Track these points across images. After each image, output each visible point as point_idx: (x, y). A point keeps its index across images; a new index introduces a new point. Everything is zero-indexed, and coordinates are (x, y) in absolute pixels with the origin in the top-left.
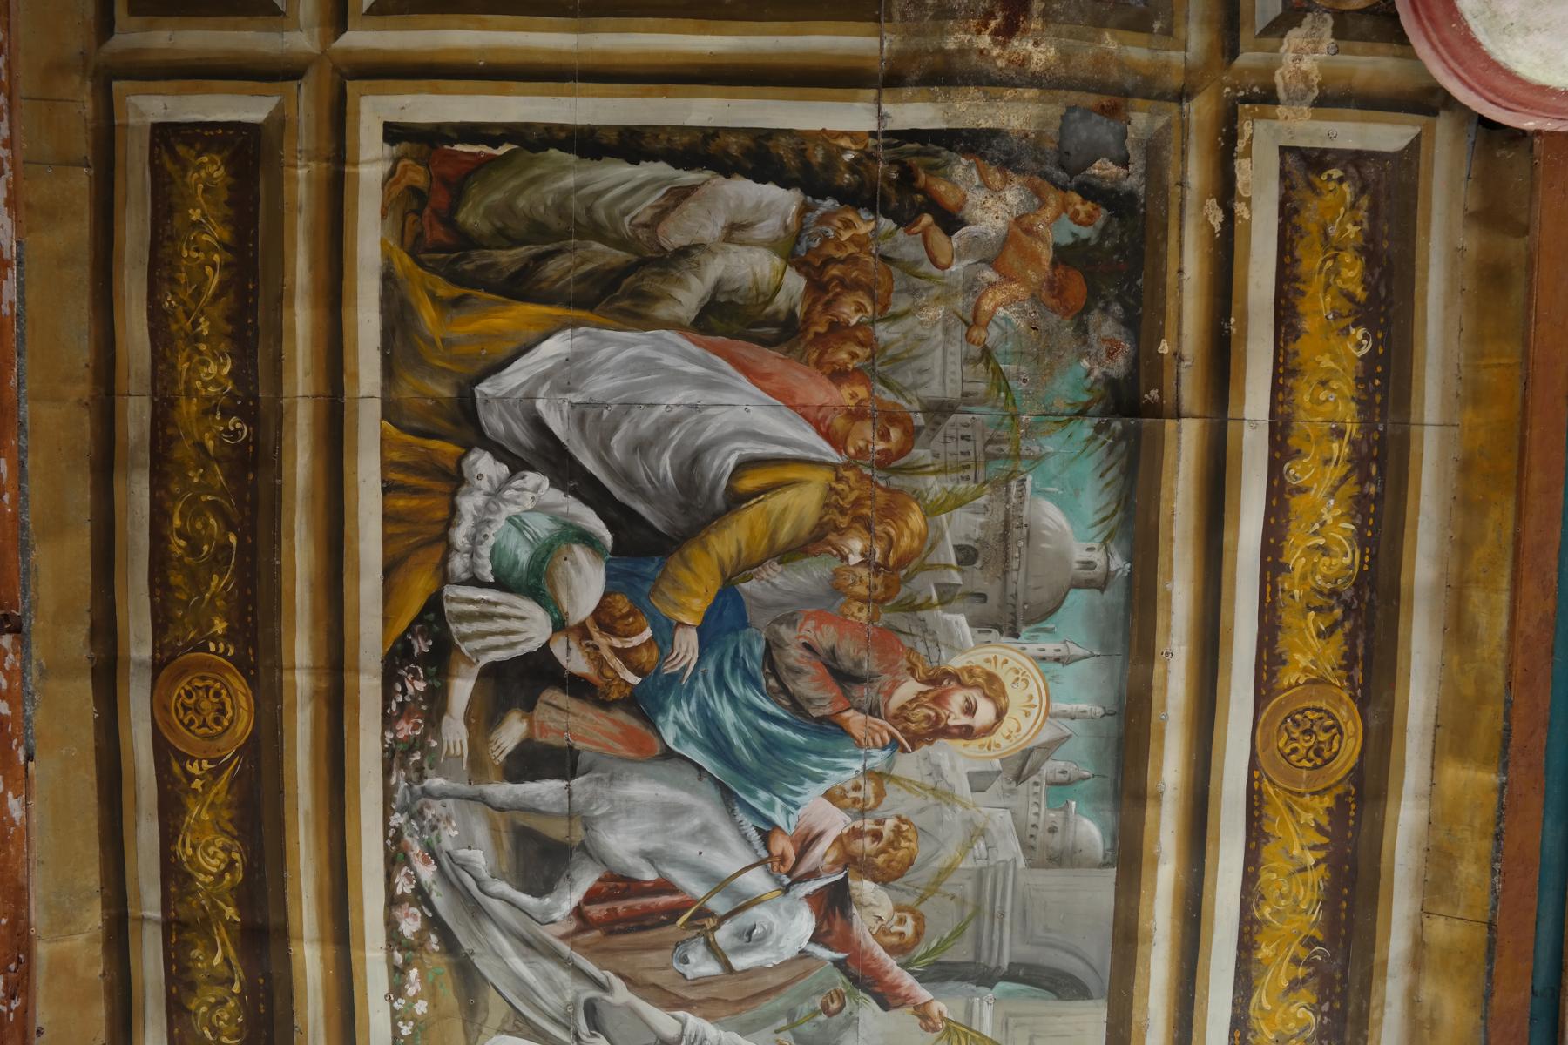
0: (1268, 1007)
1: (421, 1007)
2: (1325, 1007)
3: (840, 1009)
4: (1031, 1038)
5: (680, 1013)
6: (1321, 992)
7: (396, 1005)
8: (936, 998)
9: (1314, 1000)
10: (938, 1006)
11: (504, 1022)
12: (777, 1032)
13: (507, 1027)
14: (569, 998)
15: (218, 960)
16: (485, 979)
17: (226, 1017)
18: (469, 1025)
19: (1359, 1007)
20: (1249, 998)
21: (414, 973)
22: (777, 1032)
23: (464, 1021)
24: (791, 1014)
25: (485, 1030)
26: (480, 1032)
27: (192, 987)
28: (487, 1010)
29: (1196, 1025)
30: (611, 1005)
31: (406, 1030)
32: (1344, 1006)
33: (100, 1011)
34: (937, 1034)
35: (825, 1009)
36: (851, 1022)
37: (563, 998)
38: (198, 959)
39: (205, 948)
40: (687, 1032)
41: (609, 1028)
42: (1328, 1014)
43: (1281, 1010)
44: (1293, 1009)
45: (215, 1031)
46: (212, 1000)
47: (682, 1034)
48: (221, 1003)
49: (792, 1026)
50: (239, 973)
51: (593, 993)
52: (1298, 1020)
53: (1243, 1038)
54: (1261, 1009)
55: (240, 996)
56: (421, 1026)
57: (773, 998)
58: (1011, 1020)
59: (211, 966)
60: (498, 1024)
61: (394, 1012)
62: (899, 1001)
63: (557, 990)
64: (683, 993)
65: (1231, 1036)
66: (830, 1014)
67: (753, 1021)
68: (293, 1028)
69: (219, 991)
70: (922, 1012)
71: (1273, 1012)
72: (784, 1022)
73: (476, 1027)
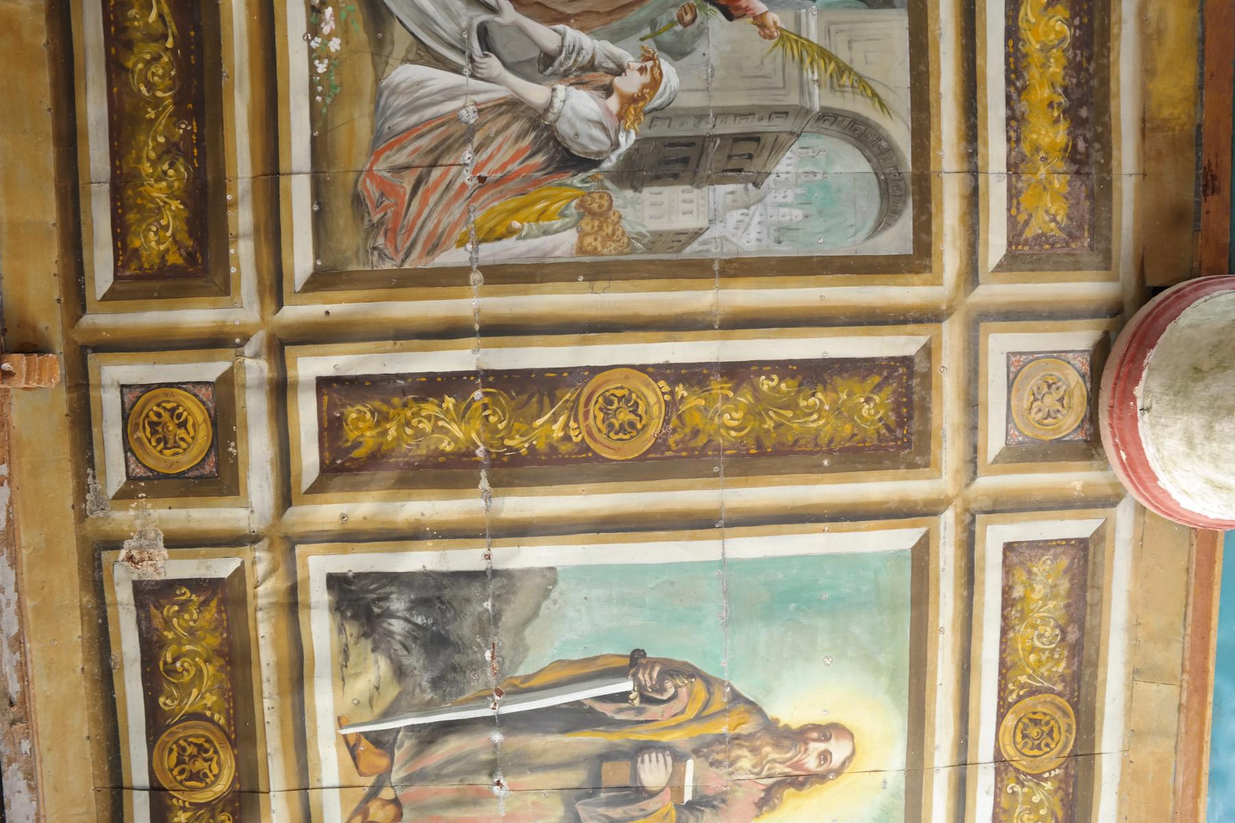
0: (1033, 20)
1: (335, 45)
2: (1077, 22)
3: (693, 20)
4: (849, 42)
5: (560, 27)
6: (1072, 8)
7: (313, 44)
8: (771, 10)
9: (1067, 14)
10: (773, 17)
11: (408, 52)
12: (642, 39)
13: (411, 56)
14: (464, 24)
15: (153, 17)
16: (391, 13)
17: (160, 72)
18: (377, 58)
19: (1102, 21)
20: (1018, 12)
21: (329, 11)
22: (642, 39)
23: (373, 54)
24: (653, 24)
25: (391, 61)
26: (387, 63)
27: (129, 45)
28: (393, 43)
29: (978, 34)
30: (501, 26)
31: (321, 68)
32: (1091, 21)
33: (44, 78)
34: (773, 42)
35: (680, 20)
36: (702, 32)
37: (458, 24)
38: (135, 19)
39: (142, 8)
40: (566, 44)
41: (499, 46)
42: (1079, 27)
43: (1043, 23)
44: (1052, 22)
45: (151, 86)
46: (148, 57)
47: (563, 46)
48: (156, 59)
49: (654, 35)
50: (173, 28)
51: (485, 17)
52: (1057, 32)
53: (1015, 46)
54: (1028, 21)
55: (173, 50)
56: (336, 62)
57: (637, 9)
58: (833, 28)
59: (147, 24)
60: (403, 54)
61: (311, 51)
62: (740, 12)
63: (453, 18)
64: (562, 9)
65: (1006, 45)
66: (685, 25)
67: (621, 30)
68: (221, 73)
69: (154, 47)
70: (760, 22)
71: (1037, 24)
72: (647, 31)
73: (383, 58)
